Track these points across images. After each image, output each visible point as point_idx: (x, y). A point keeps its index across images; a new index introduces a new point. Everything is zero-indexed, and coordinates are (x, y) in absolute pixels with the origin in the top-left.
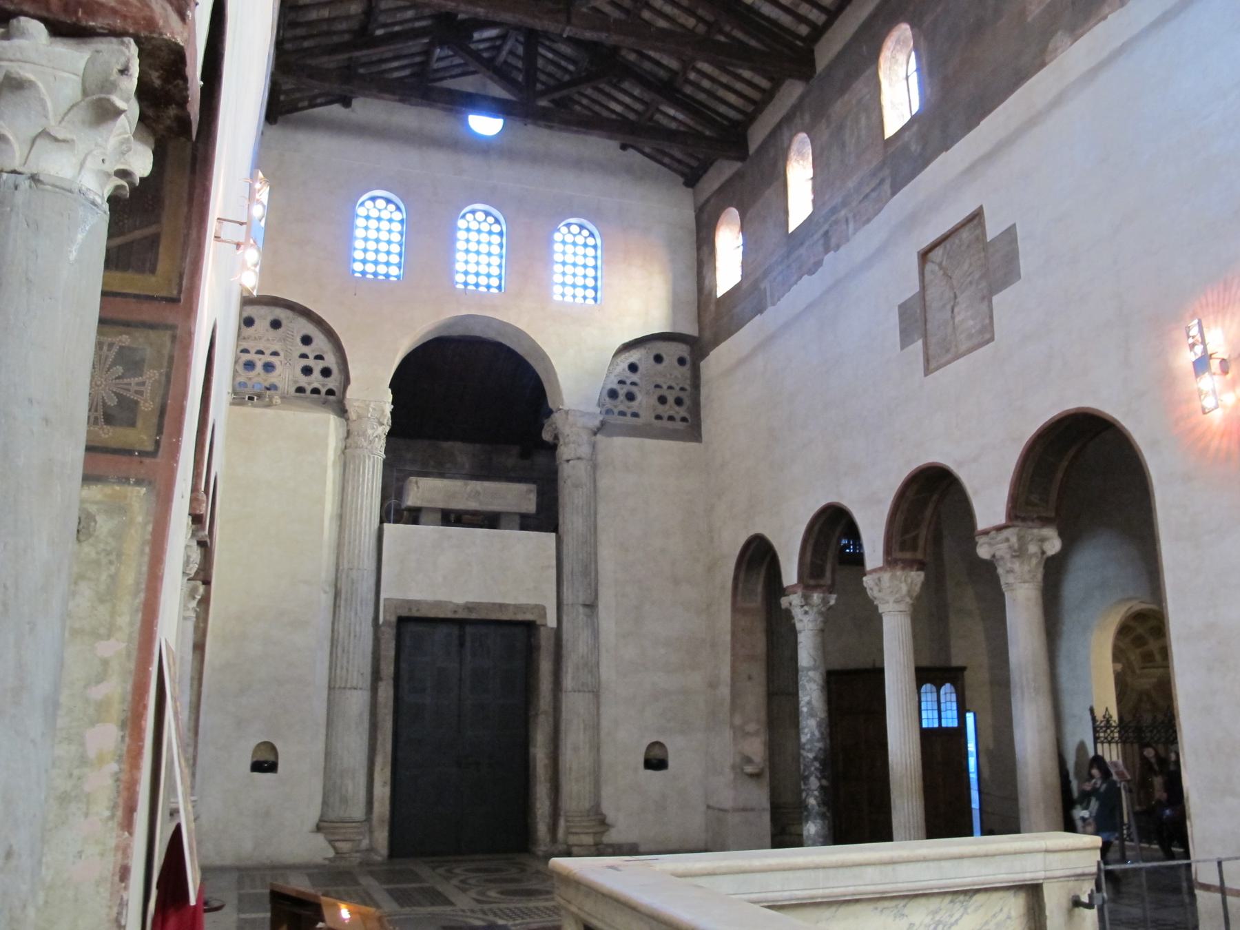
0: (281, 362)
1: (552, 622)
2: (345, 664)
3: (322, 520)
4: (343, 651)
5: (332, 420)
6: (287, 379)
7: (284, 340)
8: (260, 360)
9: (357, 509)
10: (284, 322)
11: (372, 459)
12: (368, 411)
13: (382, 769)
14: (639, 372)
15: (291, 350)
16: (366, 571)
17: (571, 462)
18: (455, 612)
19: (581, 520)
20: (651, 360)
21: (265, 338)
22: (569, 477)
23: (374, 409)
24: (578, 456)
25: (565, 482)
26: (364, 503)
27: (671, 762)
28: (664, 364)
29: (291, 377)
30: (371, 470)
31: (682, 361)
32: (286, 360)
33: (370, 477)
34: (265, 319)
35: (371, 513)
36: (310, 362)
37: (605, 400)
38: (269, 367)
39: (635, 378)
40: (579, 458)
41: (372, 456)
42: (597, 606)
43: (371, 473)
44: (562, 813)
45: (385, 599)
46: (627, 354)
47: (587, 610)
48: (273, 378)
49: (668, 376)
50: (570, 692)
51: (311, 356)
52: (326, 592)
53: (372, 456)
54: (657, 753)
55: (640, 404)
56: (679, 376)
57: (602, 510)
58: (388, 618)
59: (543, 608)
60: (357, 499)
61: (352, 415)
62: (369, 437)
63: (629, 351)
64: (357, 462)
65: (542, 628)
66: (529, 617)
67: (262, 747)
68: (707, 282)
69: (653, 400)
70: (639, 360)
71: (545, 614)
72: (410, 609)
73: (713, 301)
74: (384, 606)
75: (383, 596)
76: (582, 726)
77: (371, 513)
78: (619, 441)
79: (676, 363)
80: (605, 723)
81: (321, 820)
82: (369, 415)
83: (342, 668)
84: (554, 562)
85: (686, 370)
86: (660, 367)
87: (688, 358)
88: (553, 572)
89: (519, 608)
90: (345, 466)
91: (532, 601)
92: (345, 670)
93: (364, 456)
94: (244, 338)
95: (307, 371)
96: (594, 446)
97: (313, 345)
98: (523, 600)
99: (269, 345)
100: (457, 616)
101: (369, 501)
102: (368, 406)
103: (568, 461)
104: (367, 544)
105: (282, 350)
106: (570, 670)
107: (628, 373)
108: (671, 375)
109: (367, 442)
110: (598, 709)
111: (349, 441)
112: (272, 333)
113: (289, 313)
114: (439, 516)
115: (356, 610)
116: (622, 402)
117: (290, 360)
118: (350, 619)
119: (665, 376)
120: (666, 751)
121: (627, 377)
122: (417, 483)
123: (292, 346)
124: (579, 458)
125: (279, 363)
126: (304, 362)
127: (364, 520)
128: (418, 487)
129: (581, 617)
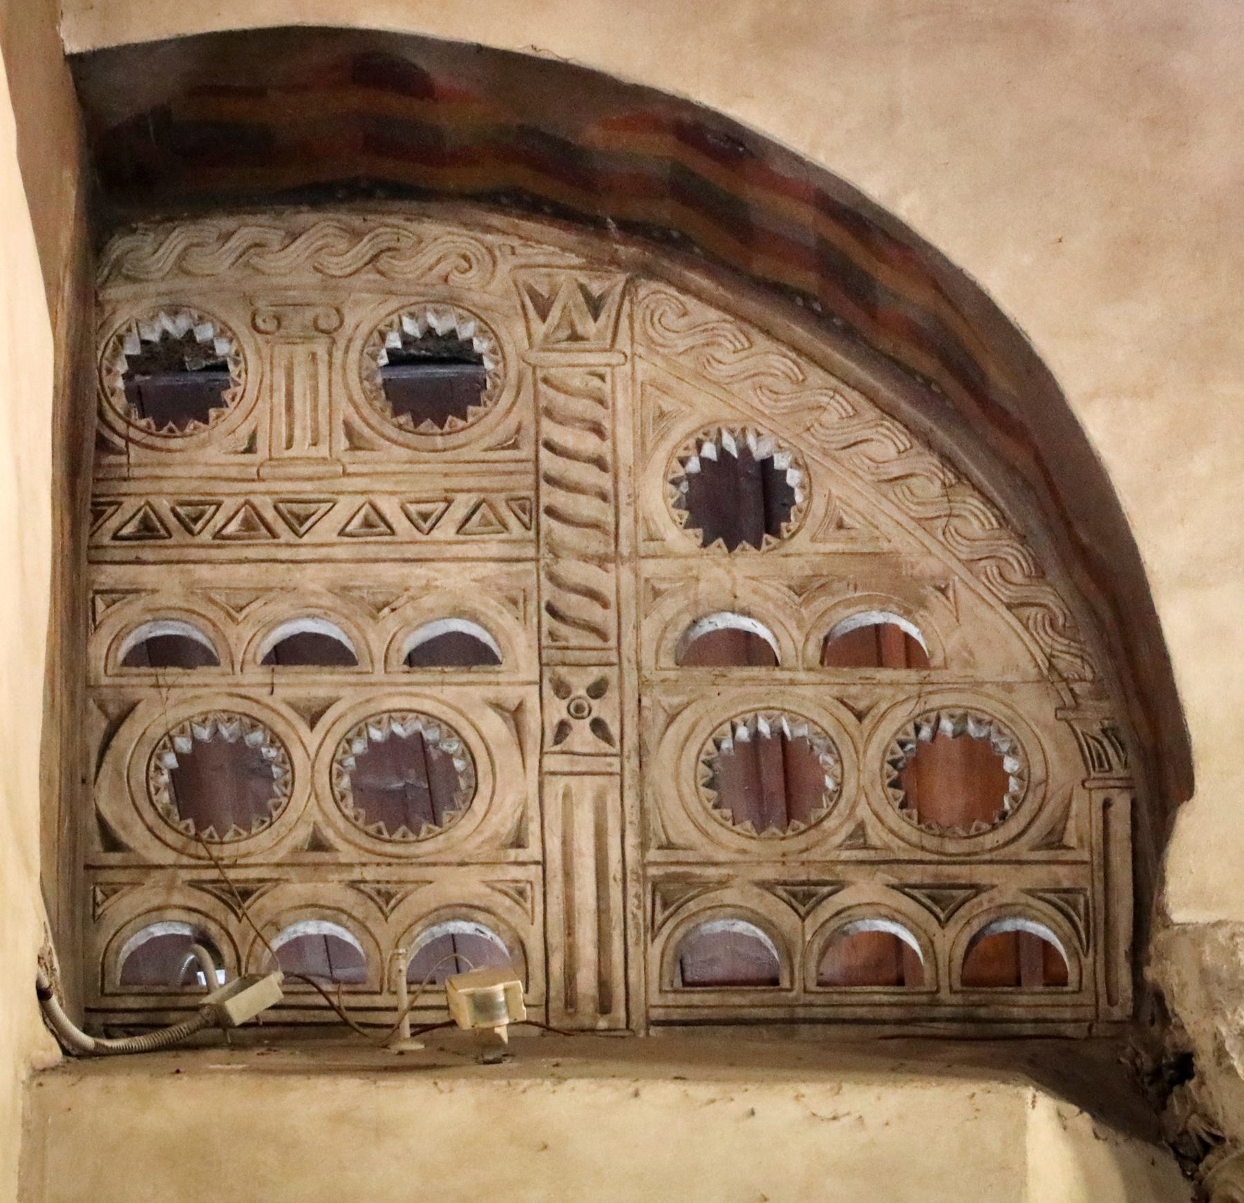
0: (514, 715)
7: (528, 510)
15: (593, 595)
32: (562, 689)
94: (149, 530)
117: (597, 690)
123: (602, 561)
125: (495, 727)
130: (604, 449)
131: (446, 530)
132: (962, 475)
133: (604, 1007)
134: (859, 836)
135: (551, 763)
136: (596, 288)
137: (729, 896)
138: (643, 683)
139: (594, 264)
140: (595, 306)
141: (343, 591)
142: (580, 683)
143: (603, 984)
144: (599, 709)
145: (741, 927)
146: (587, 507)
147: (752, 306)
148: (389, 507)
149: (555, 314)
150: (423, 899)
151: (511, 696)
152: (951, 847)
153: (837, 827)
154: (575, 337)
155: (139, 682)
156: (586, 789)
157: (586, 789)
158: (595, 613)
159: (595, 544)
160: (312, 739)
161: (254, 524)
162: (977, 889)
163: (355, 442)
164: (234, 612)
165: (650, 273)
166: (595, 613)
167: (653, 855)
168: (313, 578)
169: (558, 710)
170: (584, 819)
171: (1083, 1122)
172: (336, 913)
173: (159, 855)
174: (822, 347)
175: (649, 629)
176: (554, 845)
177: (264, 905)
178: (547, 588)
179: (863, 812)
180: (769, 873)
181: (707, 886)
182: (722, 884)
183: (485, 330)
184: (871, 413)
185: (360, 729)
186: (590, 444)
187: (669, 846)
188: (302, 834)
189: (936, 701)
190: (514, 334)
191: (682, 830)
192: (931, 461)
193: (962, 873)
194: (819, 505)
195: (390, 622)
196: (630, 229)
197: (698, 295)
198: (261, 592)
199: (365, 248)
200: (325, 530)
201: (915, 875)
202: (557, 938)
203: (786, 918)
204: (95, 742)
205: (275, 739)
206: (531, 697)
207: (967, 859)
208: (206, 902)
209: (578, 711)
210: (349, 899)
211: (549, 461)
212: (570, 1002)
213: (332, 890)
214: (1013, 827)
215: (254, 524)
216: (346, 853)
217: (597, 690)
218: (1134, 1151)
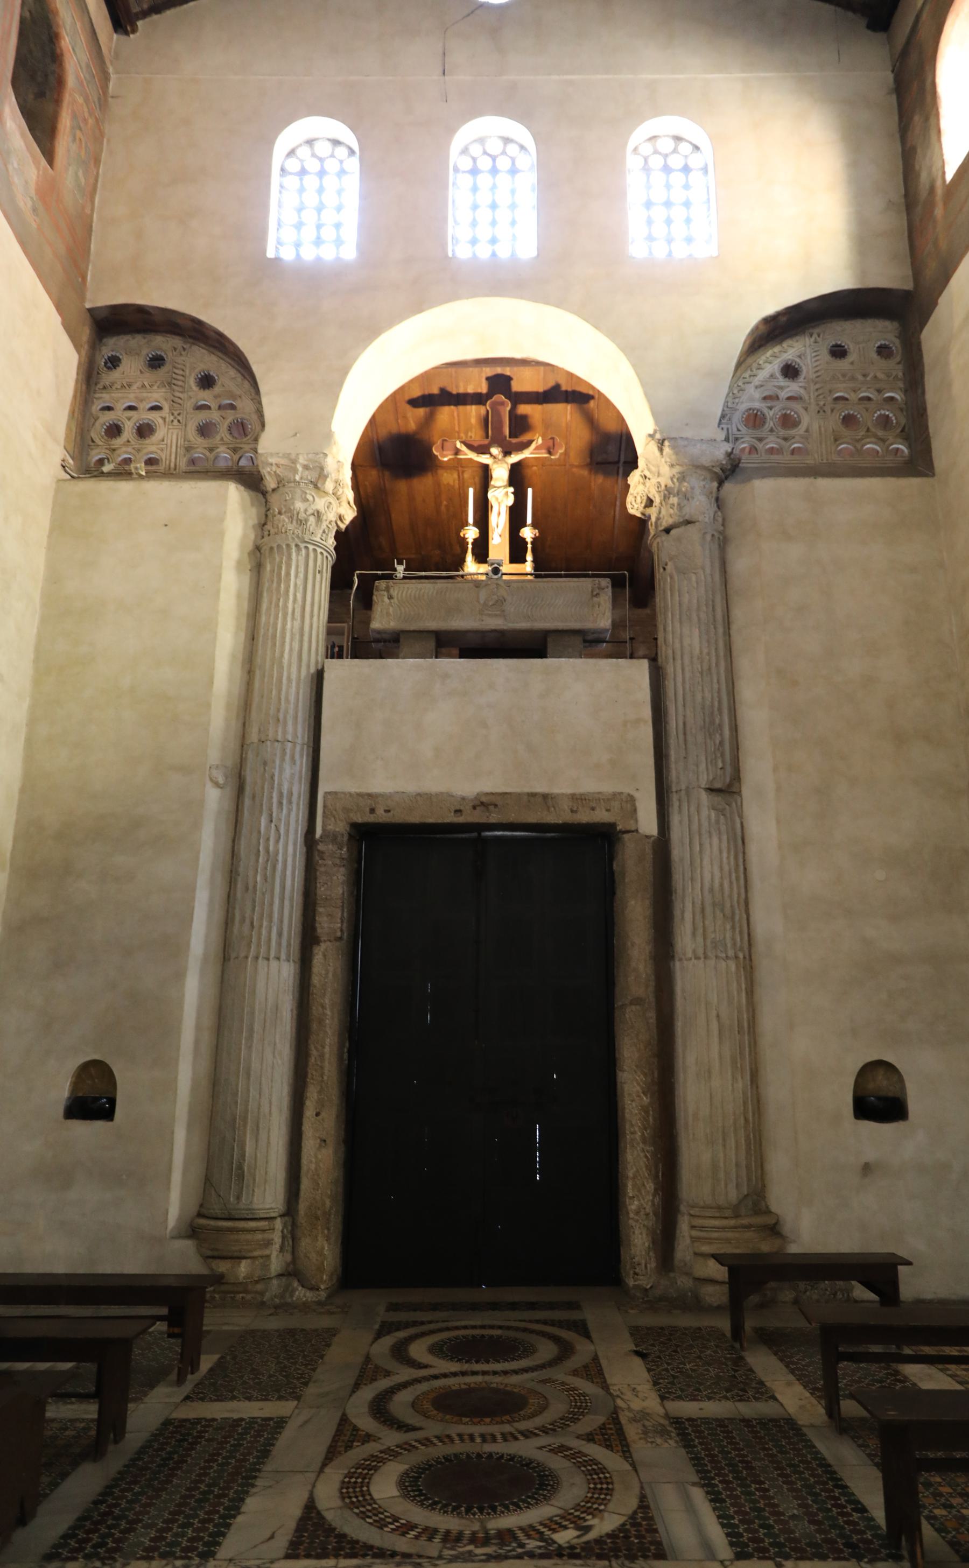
0: (164, 419)
1: (648, 823)
2: (247, 915)
3: (212, 659)
4: (247, 889)
5: (234, 492)
6: (174, 447)
7: (169, 384)
8: (129, 419)
9: (274, 636)
10: (169, 356)
11: (304, 552)
12: (295, 471)
13: (317, 1114)
14: (801, 378)
15: (179, 398)
16: (290, 744)
17: (673, 532)
18: (458, 811)
19: (696, 633)
20: (825, 356)
21: (139, 384)
22: (671, 559)
23: (306, 467)
24: (687, 517)
25: (664, 569)
26: (289, 626)
27: (913, 1106)
28: (852, 357)
29: (181, 442)
30: (302, 569)
31: (884, 351)
32: (173, 414)
33: (300, 582)
34: (138, 354)
35: (301, 641)
36: (214, 415)
37: (739, 430)
38: (144, 431)
39: (793, 387)
40: (688, 522)
41: (302, 545)
42: (739, 793)
43: (301, 575)
44: (683, 1208)
45: (326, 793)
46: (777, 349)
47: (718, 799)
48: (151, 447)
49: (860, 378)
50: (691, 959)
51: (214, 405)
52: (217, 785)
53: (302, 545)
54: (880, 1084)
55: (807, 431)
56: (880, 375)
57: (739, 614)
58: (330, 827)
59: (631, 799)
60: (276, 618)
61: (270, 483)
62: (298, 513)
63: (781, 343)
64: (277, 559)
65: (626, 837)
66: (601, 816)
67: (93, 1071)
68: (924, 176)
69: (834, 421)
70: (800, 357)
71: (635, 810)
72: (372, 811)
73: (939, 191)
74: (325, 806)
75: (323, 788)
76: (714, 1026)
77: (301, 641)
78: (763, 487)
79: (874, 355)
80: (769, 1022)
81: (200, 1215)
82: (297, 478)
83: (243, 920)
84: (647, 712)
85: (895, 367)
86: (843, 364)
87: (896, 345)
88: (646, 733)
89: (579, 799)
90: (258, 568)
91: (607, 788)
92: (248, 922)
93: (288, 546)
94: (105, 388)
95: (205, 430)
96: (719, 502)
97: (217, 389)
98: (589, 786)
99: (145, 395)
100: (461, 819)
101: (297, 624)
102: (294, 462)
103: (667, 531)
104: (292, 698)
105: (166, 399)
106: (688, 916)
107: (782, 381)
108: (865, 376)
109: (294, 522)
110: (750, 992)
111: (268, 527)
112: (149, 377)
113: (177, 341)
114: (432, 644)
115: (271, 815)
116: (772, 430)
117: (179, 414)
118: (259, 832)
119: (853, 378)
120: (901, 1080)
121: (781, 388)
122: (387, 589)
123: (182, 392)
124: (688, 522)
125: (160, 421)
126: (203, 416)
127: (286, 655)
128: (390, 597)
129: (705, 812)
130: (184, 374)
131: (155, 387)
132: (245, 377)
133: (175, 469)
134: (222, 439)
135: (170, 427)
136: (185, 346)
137: (198, 450)
138: (187, 413)
139: (185, 342)
140: (184, 349)
141: (136, 398)
142: (176, 413)
143: (175, 465)
144: (179, 418)
145: (201, 455)
146: (180, 383)
147: (212, 349)
148: (146, 384)
149: (177, 351)
150: (145, 451)
151: (163, 415)
152: (238, 441)
153: (218, 438)
154: (181, 355)
155: (100, 414)
156: (175, 432)
157: (175, 432)
158: (180, 401)
159: (181, 389)
160: (128, 423)
161: (123, 386)
162: (241, 448)
163: (141, 372)
164: (117, 401)
165: (194, 344)
166: (180, 401)
167: (186, 443)
168: (132, 396)
169: (172, 418)
170: (175, 437)
171: (242, 488)
172: (130, 453)
173: (100, 443)
174: (224, 357)
175: (189, 404)
176: (169, 441)
177: (117, 452)
178: (172, 398)
179: (223, 435)
180: (206, 446)
181: (194, 448)
182: (197, 448)
183: (166, 354)
184: (230, 367)
185: (138, 421)
186: (181, 372)
187: (189, 441)
188: (125, 440)
189: (238, 416)
190: (170, 354)
191: (192, 439)
192: (239, 375)
193: (237, 445)
194: (220, 383)
195: (144, 403)
196: (190, 337)
197: (203, 348)
198: (123, 398)
199: (146, 340)
200: (135, 387)
201: (231, 446)
202: (168, 457)
203: (208, 453)
204: (91, 424)
205: (122, 423)
206: (167, 415)
207: (241, 443)
208: (107, 451)
209: (175, 418)
210: (133, 451)
211: (174, 375)
212: (170, 469)
213: (130, 449)
214: (249, 437)
215: (123, 386)
216: (132, 443)
217: (179, 414)
218: (253, 494)
